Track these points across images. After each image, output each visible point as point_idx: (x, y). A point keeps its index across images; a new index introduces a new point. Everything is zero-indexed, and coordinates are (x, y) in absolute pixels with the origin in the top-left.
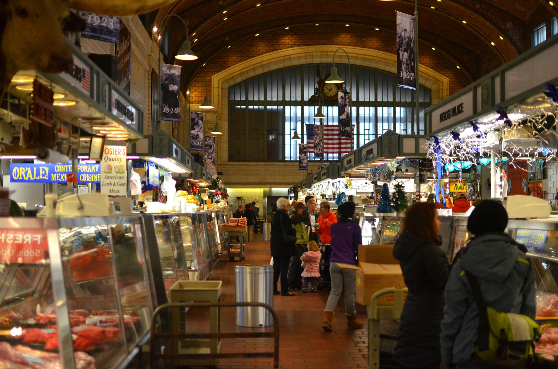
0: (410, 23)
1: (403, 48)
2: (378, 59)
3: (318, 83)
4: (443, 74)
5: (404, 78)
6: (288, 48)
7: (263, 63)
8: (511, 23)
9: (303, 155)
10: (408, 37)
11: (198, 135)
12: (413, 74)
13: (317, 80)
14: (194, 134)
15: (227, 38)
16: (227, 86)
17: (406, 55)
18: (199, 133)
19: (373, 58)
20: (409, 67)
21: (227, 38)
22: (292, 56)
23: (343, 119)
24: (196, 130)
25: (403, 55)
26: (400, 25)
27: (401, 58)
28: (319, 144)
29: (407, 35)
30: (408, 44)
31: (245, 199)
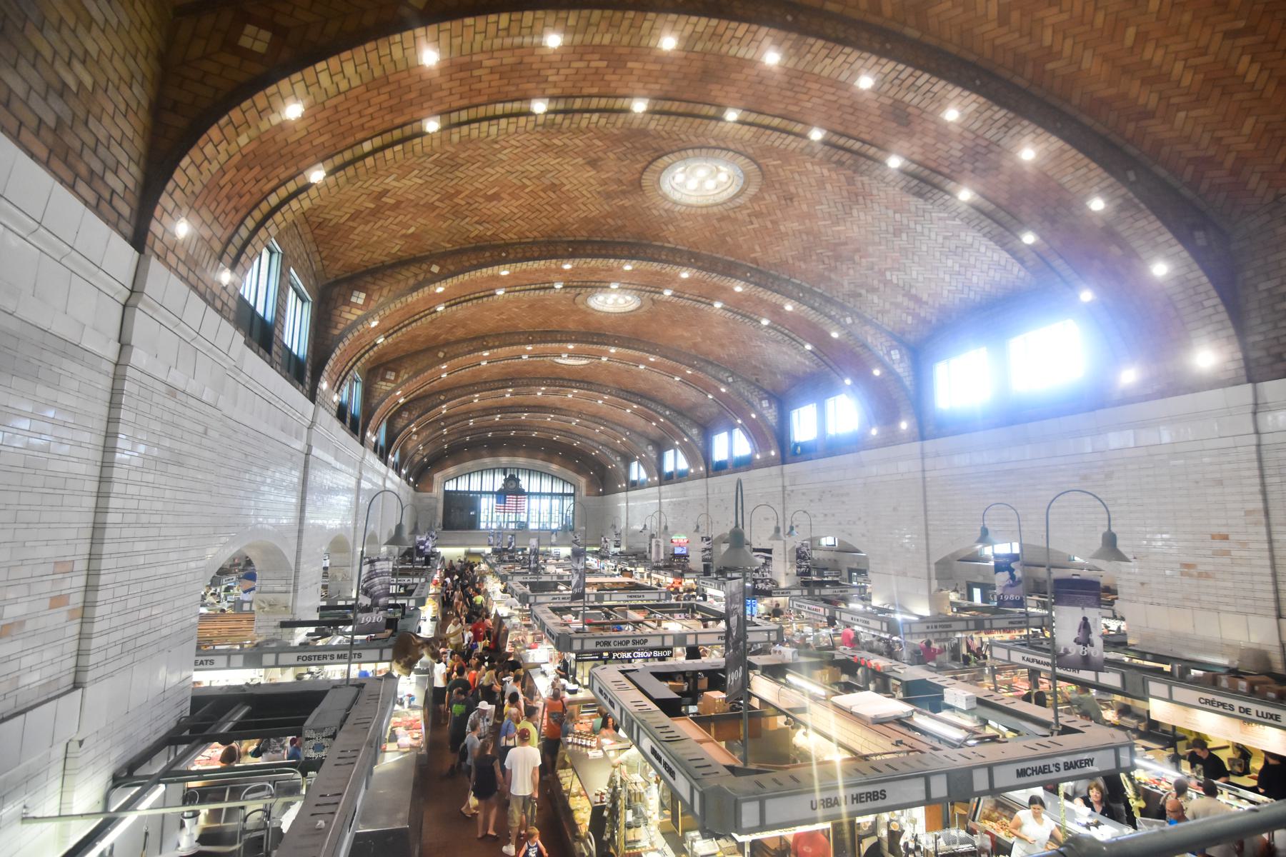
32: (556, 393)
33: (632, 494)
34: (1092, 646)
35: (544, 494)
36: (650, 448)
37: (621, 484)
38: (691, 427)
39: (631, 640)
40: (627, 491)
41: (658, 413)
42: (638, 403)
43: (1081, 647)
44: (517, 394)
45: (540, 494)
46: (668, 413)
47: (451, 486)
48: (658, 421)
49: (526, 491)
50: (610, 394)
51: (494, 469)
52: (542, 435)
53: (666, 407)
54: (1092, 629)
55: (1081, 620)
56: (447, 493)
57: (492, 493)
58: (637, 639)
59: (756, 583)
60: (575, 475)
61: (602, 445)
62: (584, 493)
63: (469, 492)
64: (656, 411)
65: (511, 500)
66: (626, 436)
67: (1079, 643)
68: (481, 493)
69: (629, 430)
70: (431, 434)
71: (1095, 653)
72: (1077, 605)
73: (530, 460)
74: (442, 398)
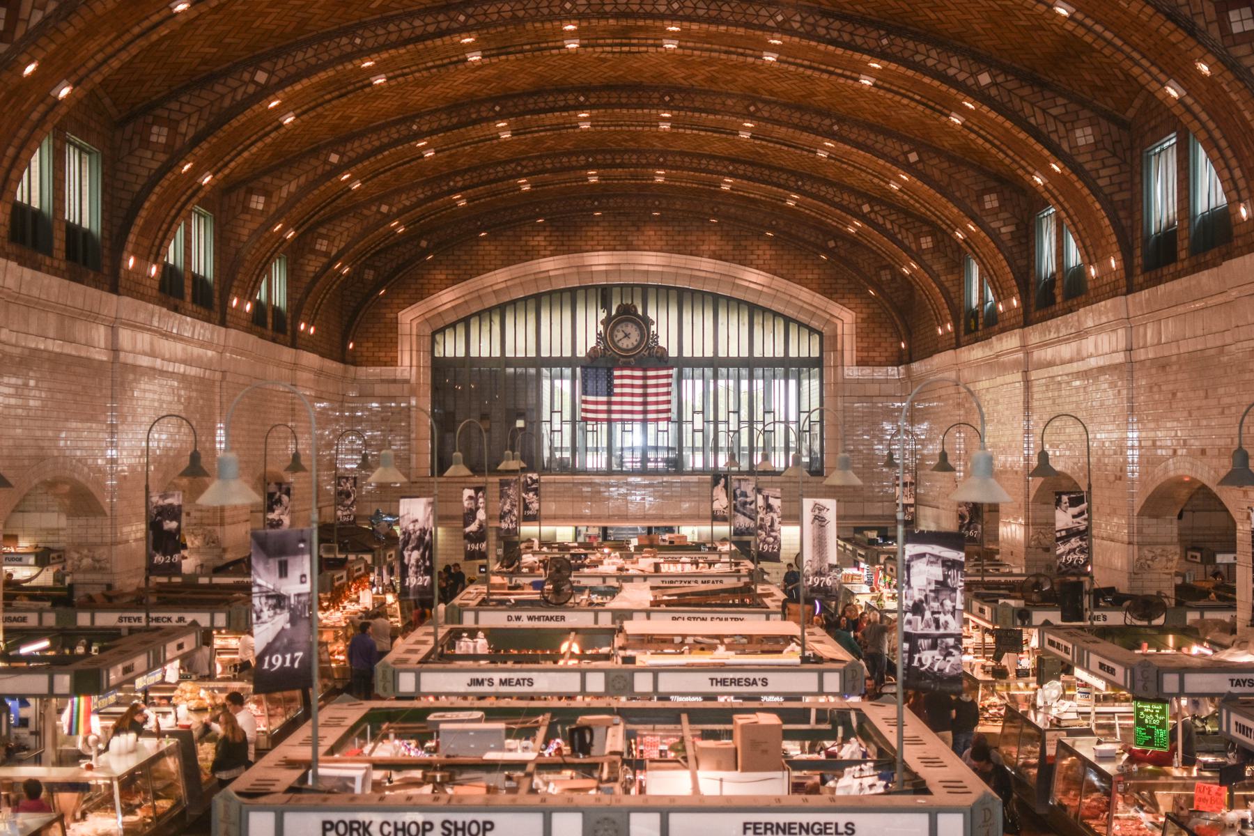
1: (410, 547)
2: (717, 277)
3: (602, 322)
4: (844, 305)
6: (545, 256)
7: (496, 287)
8: (929, 239)
9: (531, 494)
12: (428, 578)
13: (603, 315)
15: (424, 244)
16: (428, 331)
17: (416, 554)
19: (708, 275)
21: (424, 244)
22: (551, 273)
24: (277, 512)
27: (406, 561)
28: (510, 512)
29: (418, 526)
30: (421, 539)
32: (624, 33)
33: (976, 352)
35: (729, 362)
36: (991, 202)
37: (943, 325)
38: (1070, 123)
40: (958, 345)
41: (951, 81)
42: (881, 55)
44: (502, 51)
45: (715, 364)
46: (985, 79)
47: (451, 347)
48: (963, 111)
49: (673, 353)
50: (782, 29)
51: (573, 292)
52: (687, 179)
53: (982, 60)
56: (441, 369)
57: (571, 362)
59: (914, 649)
60: (819, 300)
61: (871, 200)
62: (849, 355)
63: (505, 361)
64: (951, 81)
65: (626, 380)
66: (909, 168)
68: (539, 362)
69: (918, 147)
70: (304, 190)
73: (678, 260)
74: (261, 77)
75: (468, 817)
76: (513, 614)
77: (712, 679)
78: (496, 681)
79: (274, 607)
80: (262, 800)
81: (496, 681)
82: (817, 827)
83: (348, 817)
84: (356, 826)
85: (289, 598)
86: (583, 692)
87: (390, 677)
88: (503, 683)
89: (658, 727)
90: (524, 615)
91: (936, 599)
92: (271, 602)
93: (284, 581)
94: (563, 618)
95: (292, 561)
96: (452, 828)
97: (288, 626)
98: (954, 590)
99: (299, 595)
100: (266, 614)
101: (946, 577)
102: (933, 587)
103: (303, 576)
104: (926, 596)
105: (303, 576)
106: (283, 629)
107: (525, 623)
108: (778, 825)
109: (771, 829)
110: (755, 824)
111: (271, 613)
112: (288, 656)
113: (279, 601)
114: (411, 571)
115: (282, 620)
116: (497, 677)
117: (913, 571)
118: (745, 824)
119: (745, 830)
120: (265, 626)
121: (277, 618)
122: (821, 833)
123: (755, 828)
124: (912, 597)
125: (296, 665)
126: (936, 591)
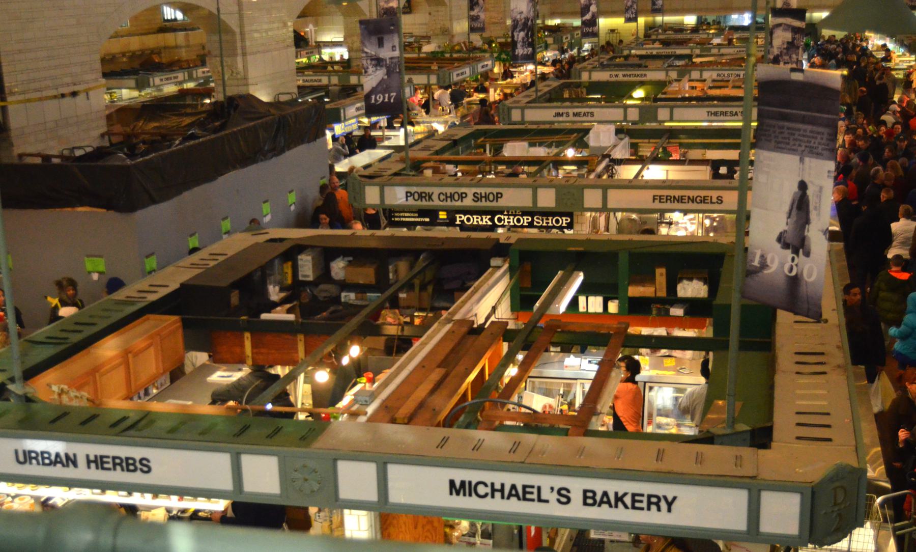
0: (528, 5)
1: (518, 29)
5: (520, 55)
10: (525, 18)
11: (478, 16)
12: (530, 49)
14: (473, 16)
17: (522, 34)
18: (479, 14)
20: (527, 43)
23: (586, 20)
25: (518, 35)
26: (515, 10)
27: (516, 39)
28: (631, 6)
29: (523, 16)
30: (525, 24)
31: (621, 32)
34: (807, 254)
39: (470, 191)
43: (789, 254)
54: (813, 215)
55: (795, 188)
58: (482, 191)
67: (786, 246)
71: (810, 276)
72: (793, 151)
75: (488, 190)
76: (614, 73)
77: (708, 112)
78: (571, 114)
79: (376, 66)
80: (377, 180)
81: (571, 114)
82: (699, 198)
83: (420, 190)
84: (424, 195)
85: (386, 60)
86: (625, 120)
87: (506, 110)
88: (575, 115)
89: (651, 141)
90: (621, 73)
91: (787, 54)
92: (373, 62)
93: (382, 50)
94: (645, 75)
95: (386, 37)
96: (479, 196)
97: (386, 77)
98: (798, 48)
99: (391, 58)
100: (371, 70)
101: (793, 39)
102: (785, 46)
103: (394, 47)
104: (781, 52)
105: (394, 47)
106: (383, 79)
107: (620, 78)
108: (674, 197)
109: (670, 199)
110: (660, 196)
111: (374, 69)
112: (387, 95)
113: (378, 62)
114: (519, 45)
115: (381, 74)
116: (571, 111)
117: (775, 35)
118: (654, 196)
119: (654, 199)
120: (371, 77)
121: (378, 72)
122: (701, 202)
123: (660, 199)
124: (773, 52)
125: (392, 101)
126: (787, 49)
